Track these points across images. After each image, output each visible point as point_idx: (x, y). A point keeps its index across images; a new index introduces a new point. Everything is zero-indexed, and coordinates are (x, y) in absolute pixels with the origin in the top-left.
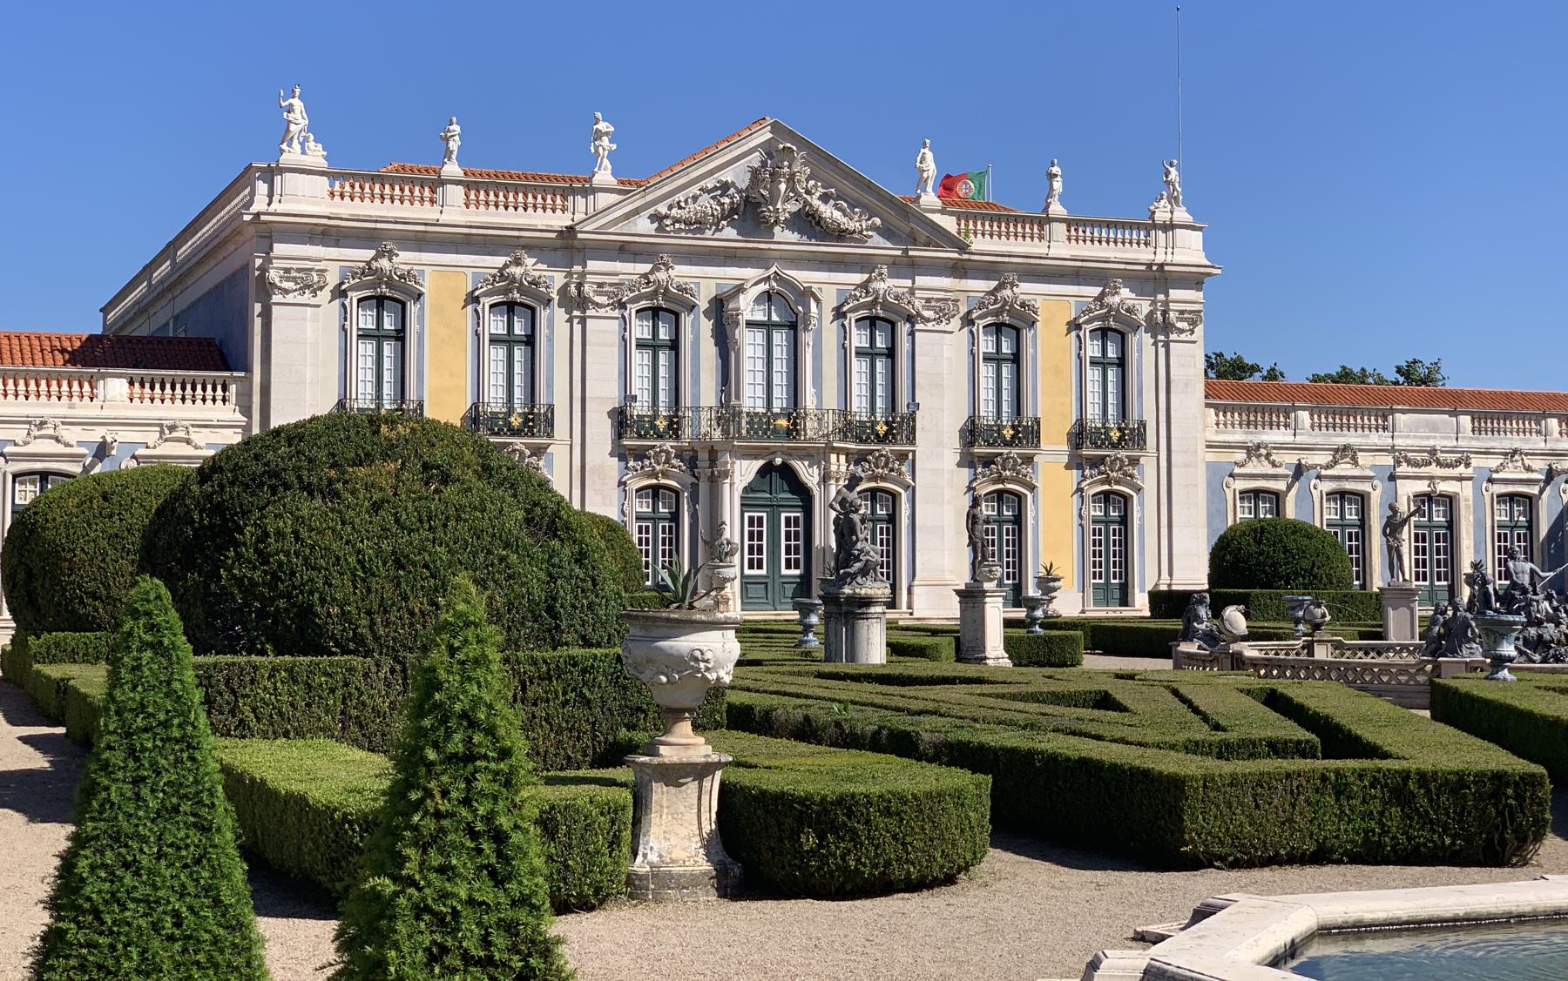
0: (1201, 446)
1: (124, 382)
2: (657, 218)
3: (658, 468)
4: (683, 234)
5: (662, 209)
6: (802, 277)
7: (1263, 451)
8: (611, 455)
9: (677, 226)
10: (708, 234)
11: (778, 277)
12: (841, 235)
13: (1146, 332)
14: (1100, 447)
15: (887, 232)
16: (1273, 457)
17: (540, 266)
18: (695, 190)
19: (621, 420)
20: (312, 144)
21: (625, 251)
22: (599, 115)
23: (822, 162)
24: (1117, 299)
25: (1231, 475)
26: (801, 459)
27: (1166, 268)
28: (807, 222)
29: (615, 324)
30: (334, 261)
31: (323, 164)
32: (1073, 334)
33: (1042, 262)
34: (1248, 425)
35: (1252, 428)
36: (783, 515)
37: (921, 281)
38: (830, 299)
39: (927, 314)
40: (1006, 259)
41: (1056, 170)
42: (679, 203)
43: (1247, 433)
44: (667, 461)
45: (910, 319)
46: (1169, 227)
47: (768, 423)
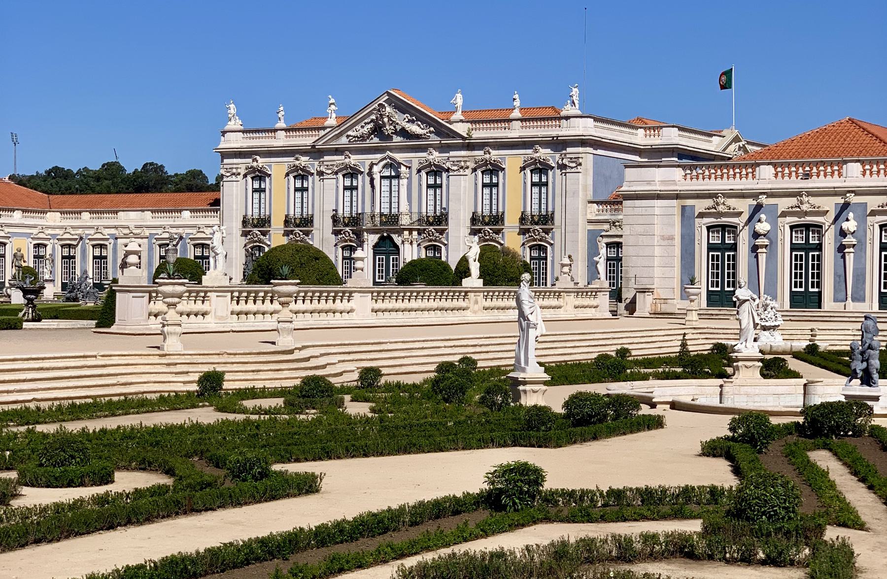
2: (348, 136)
3: (347, 238)
4: (358, 142)
5: (350, 133)
6: (399, 157)
7: (617, 224)
8: (332, 233)
9: (354, 139)
10: (368, 141)
11: (390, 158)
12: (418, 137)
13: (558, 169)
15: (438, 133)
17: (311, 160)
19: (335, 220)
20: (238, 121)
21: (338, 151)
22: (330, 97)
23: (402, 107)
24: (538, 155)
25: (601, 236)
26: (394, 233)
27: (559, 138)
28: (404, 133)
30: (242, 164)
32: (474, 173)
33: (503, 140)
36: (391, 257)
37: (452, 153)
38: (415, 166)
40: (487, 141)
41: (516, 96)
44: (349, 235)
45: (448, 170)
46: (567, 118)
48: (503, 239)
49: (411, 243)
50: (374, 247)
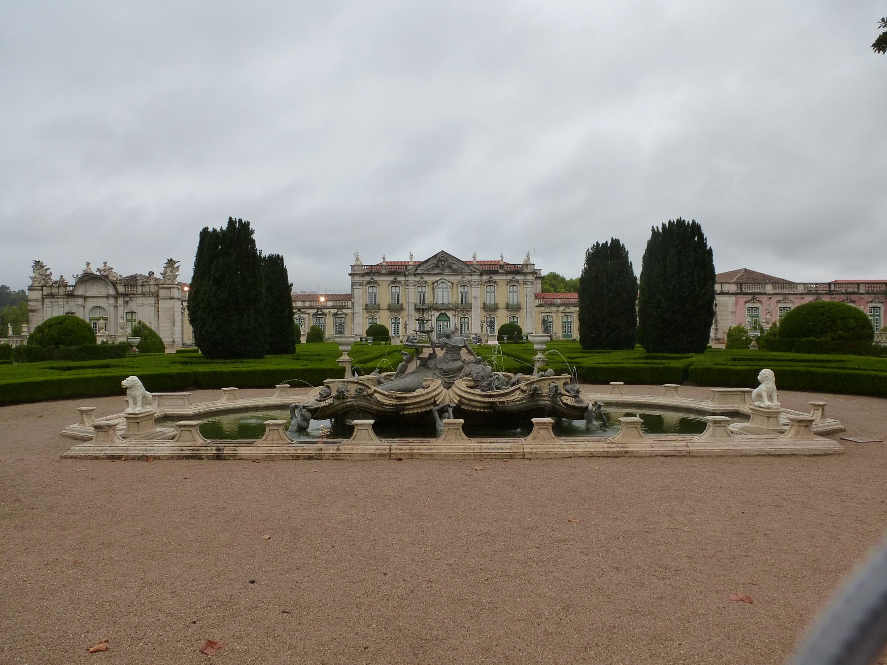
0: (534, 307)
49: (455, 316)
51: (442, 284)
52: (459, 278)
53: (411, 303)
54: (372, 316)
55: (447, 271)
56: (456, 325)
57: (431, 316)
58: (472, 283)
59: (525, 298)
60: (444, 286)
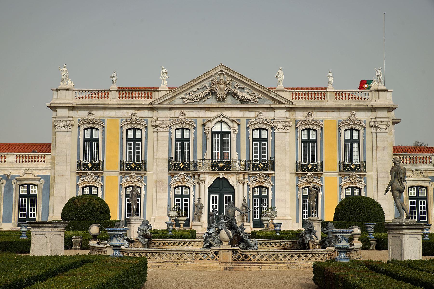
1: (15, 156)
5: (183, 96)
9: (188, 101)
14: (347, 171)
16: (424, 174)
18: (195, 89)
22: (163, 67)
29: (167, 134)
31: (73, 88)
34: (413, 162)
35: (415, 163)
36: (225, 195)
39: (279, 126)
42: (189, 94)
43: (412, 165)
47: (216, 165)
48: (322, 182)
50: (209, 187)
51: (219, 125)
52: (251, 114)
53: (163, 159)
54: (89, 182)
55: (230, 101)
56: (244, 200)
57: (199, 184)
58: (275, 123)
59: (374, 153)
60: (224, 129)
